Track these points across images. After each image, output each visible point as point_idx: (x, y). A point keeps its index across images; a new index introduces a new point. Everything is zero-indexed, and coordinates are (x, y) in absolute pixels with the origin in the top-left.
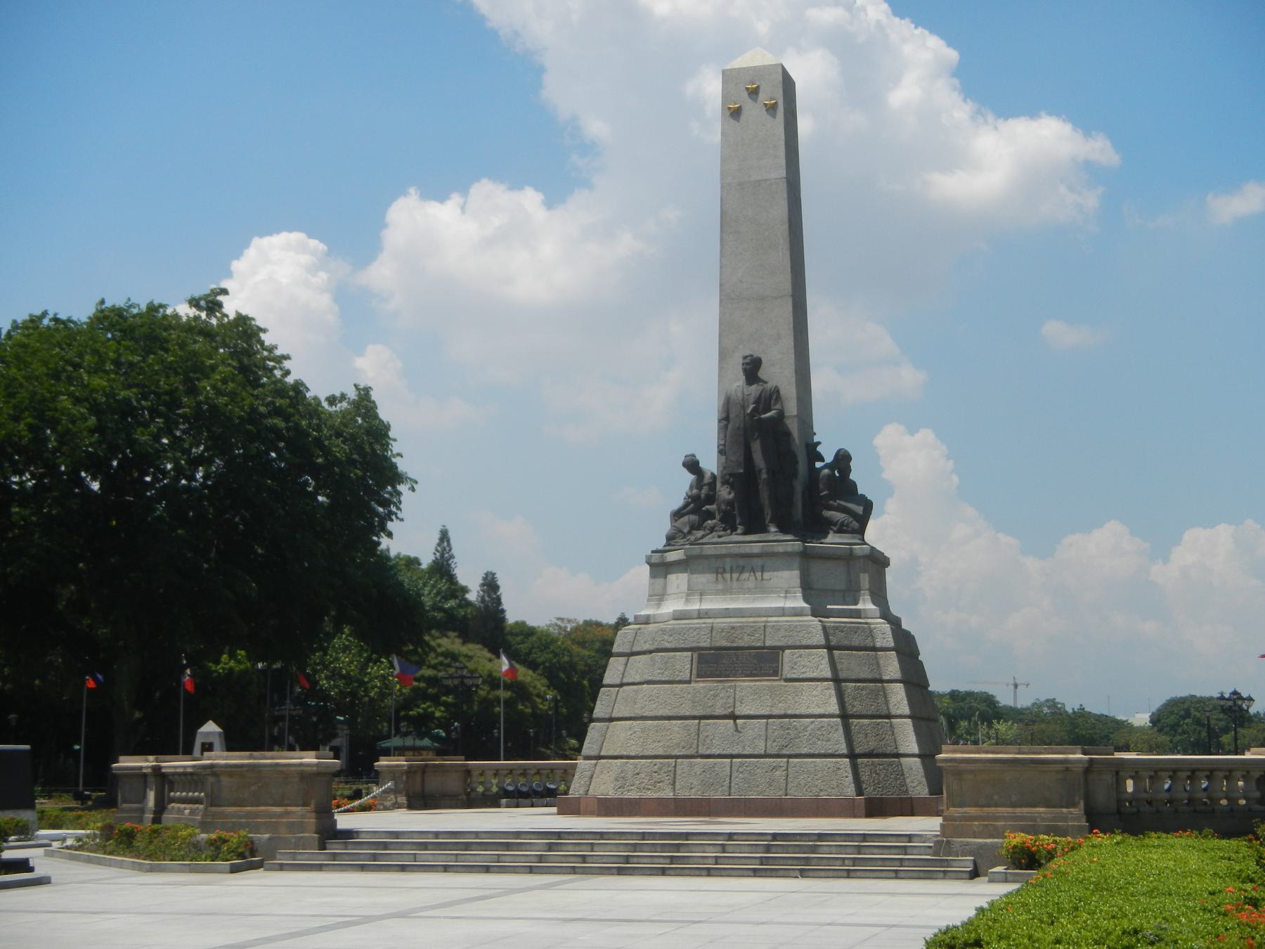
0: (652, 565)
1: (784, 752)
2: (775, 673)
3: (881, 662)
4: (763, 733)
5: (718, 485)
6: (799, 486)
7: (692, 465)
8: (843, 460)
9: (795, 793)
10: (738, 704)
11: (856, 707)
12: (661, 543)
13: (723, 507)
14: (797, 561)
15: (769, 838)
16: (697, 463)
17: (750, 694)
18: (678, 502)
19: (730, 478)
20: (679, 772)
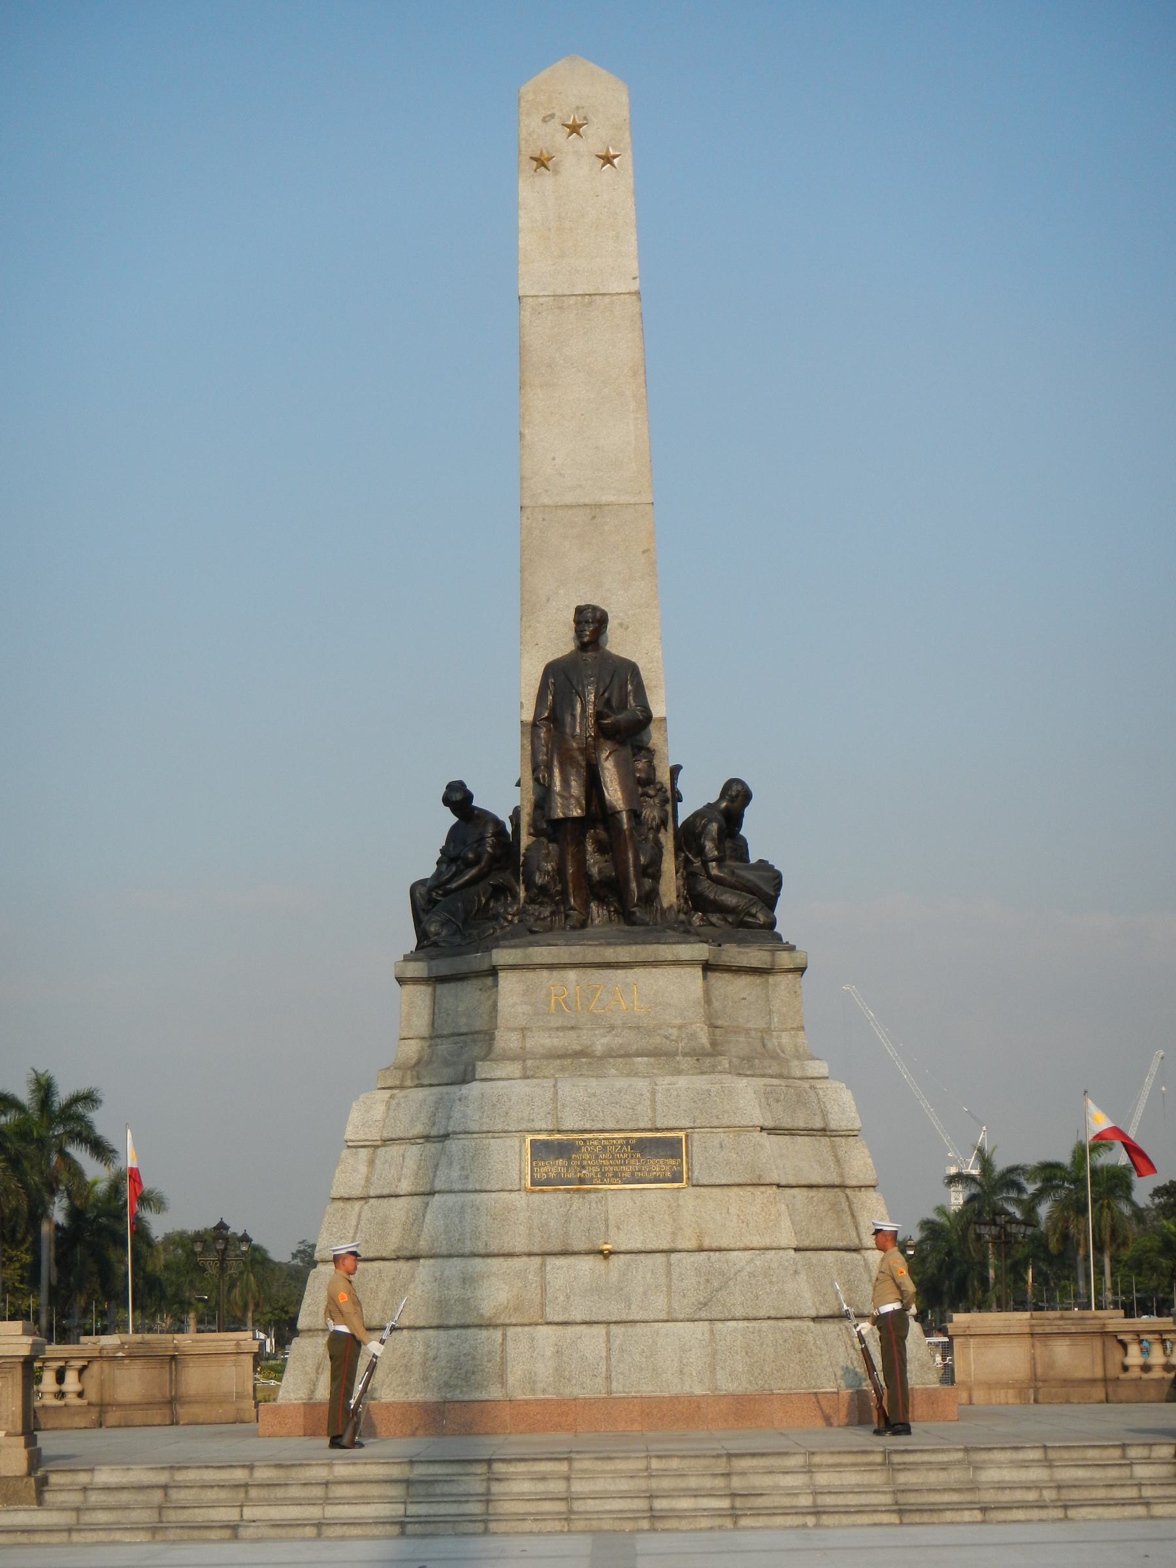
0: (401, 981)
1: (703, 1315)
2: (676, 1178)
3: (841, 1153)
4: (663, 1280)
5: (525, 840)
6: (667, 840)
7: (458, 798)
8: (736, 797)
9: (727, 1385)
10: (613, 1230)
11: (817, 1237)
12: (410, 941)
13: (539, 879)
14: (698, 972)
15: (878, 1458)
16: (469, 797)
17: (632, 1210)
18: (428, 870)
19: (550, 828)
20: (511, 1352)
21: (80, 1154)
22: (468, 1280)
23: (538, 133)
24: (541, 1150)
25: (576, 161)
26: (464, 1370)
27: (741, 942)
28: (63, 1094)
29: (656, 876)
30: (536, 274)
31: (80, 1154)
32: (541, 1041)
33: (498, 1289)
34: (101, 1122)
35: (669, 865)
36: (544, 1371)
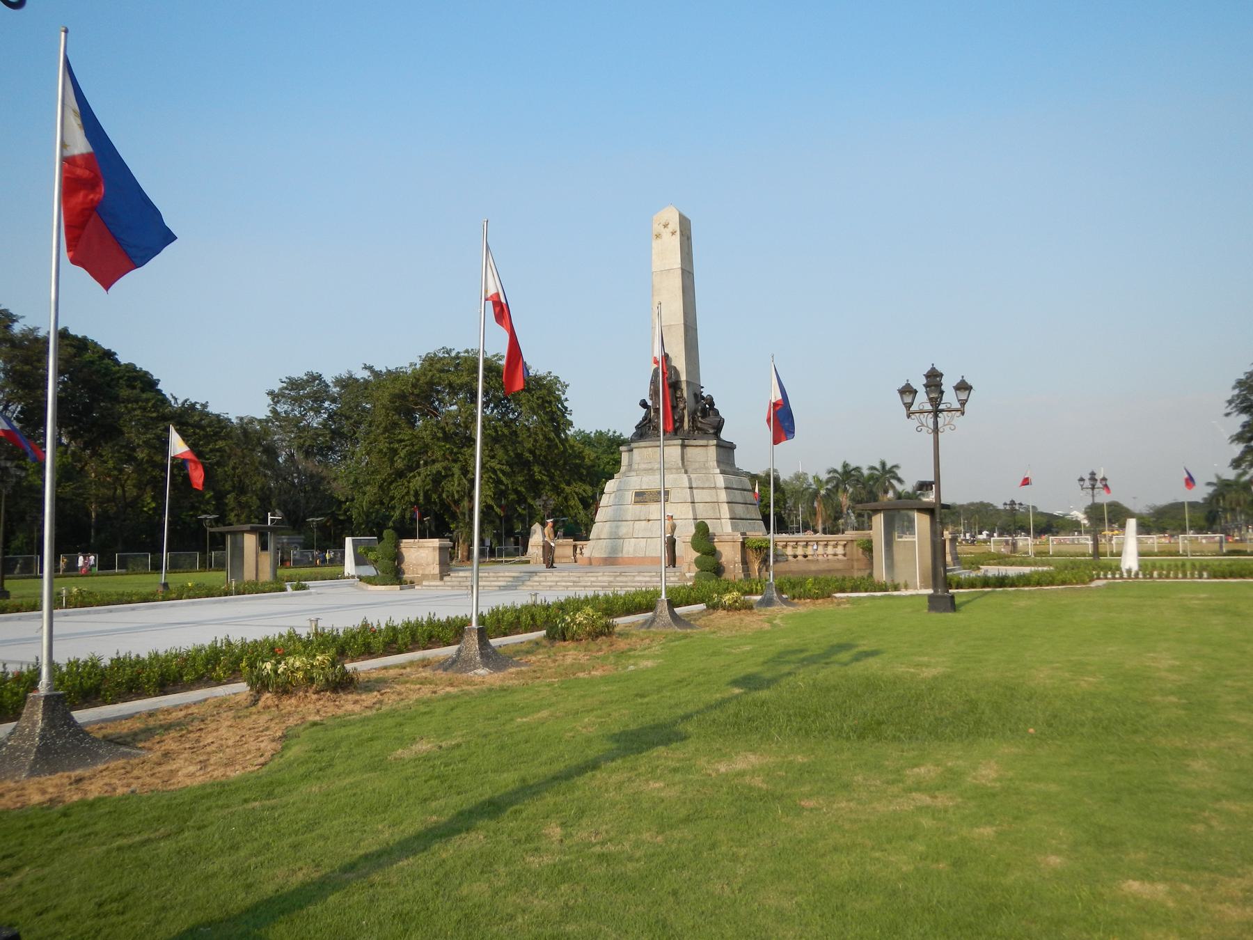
7: (644, 404)
21: (894, 482)
22: (617, 527)
23: (657, 228)
24: (638, 494)
25: (666, 233)
26: (614, 549)
27: (702, 438)
28: (888, 466)
29: (682, 421)
30: (657, 265)
31: (894, 482)
32: (643, 466)
33: (624, 529)
34: (900, 473)
35: (686, 419)
36: (631, 550)
